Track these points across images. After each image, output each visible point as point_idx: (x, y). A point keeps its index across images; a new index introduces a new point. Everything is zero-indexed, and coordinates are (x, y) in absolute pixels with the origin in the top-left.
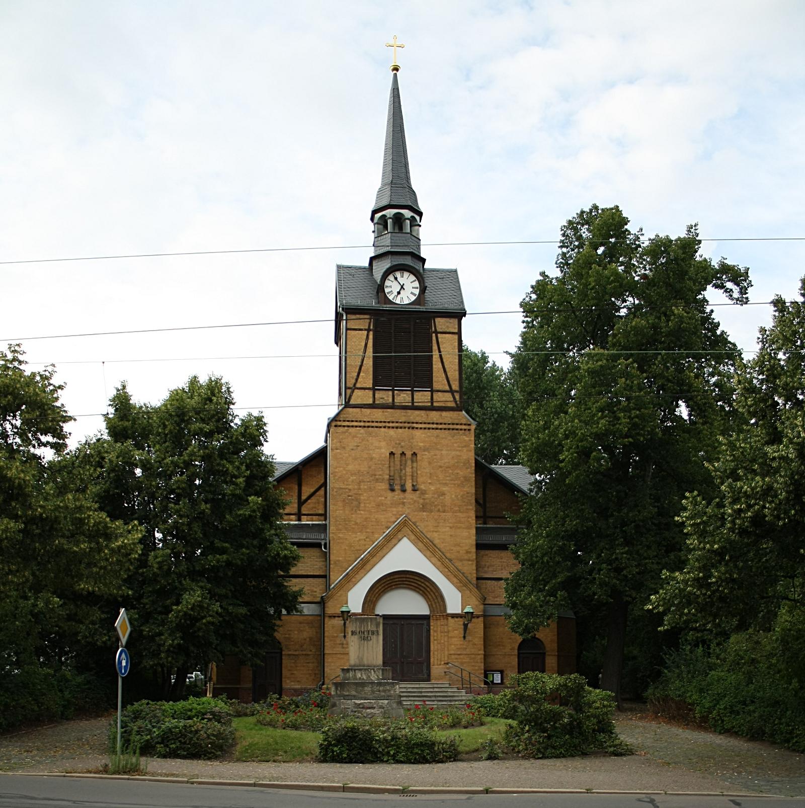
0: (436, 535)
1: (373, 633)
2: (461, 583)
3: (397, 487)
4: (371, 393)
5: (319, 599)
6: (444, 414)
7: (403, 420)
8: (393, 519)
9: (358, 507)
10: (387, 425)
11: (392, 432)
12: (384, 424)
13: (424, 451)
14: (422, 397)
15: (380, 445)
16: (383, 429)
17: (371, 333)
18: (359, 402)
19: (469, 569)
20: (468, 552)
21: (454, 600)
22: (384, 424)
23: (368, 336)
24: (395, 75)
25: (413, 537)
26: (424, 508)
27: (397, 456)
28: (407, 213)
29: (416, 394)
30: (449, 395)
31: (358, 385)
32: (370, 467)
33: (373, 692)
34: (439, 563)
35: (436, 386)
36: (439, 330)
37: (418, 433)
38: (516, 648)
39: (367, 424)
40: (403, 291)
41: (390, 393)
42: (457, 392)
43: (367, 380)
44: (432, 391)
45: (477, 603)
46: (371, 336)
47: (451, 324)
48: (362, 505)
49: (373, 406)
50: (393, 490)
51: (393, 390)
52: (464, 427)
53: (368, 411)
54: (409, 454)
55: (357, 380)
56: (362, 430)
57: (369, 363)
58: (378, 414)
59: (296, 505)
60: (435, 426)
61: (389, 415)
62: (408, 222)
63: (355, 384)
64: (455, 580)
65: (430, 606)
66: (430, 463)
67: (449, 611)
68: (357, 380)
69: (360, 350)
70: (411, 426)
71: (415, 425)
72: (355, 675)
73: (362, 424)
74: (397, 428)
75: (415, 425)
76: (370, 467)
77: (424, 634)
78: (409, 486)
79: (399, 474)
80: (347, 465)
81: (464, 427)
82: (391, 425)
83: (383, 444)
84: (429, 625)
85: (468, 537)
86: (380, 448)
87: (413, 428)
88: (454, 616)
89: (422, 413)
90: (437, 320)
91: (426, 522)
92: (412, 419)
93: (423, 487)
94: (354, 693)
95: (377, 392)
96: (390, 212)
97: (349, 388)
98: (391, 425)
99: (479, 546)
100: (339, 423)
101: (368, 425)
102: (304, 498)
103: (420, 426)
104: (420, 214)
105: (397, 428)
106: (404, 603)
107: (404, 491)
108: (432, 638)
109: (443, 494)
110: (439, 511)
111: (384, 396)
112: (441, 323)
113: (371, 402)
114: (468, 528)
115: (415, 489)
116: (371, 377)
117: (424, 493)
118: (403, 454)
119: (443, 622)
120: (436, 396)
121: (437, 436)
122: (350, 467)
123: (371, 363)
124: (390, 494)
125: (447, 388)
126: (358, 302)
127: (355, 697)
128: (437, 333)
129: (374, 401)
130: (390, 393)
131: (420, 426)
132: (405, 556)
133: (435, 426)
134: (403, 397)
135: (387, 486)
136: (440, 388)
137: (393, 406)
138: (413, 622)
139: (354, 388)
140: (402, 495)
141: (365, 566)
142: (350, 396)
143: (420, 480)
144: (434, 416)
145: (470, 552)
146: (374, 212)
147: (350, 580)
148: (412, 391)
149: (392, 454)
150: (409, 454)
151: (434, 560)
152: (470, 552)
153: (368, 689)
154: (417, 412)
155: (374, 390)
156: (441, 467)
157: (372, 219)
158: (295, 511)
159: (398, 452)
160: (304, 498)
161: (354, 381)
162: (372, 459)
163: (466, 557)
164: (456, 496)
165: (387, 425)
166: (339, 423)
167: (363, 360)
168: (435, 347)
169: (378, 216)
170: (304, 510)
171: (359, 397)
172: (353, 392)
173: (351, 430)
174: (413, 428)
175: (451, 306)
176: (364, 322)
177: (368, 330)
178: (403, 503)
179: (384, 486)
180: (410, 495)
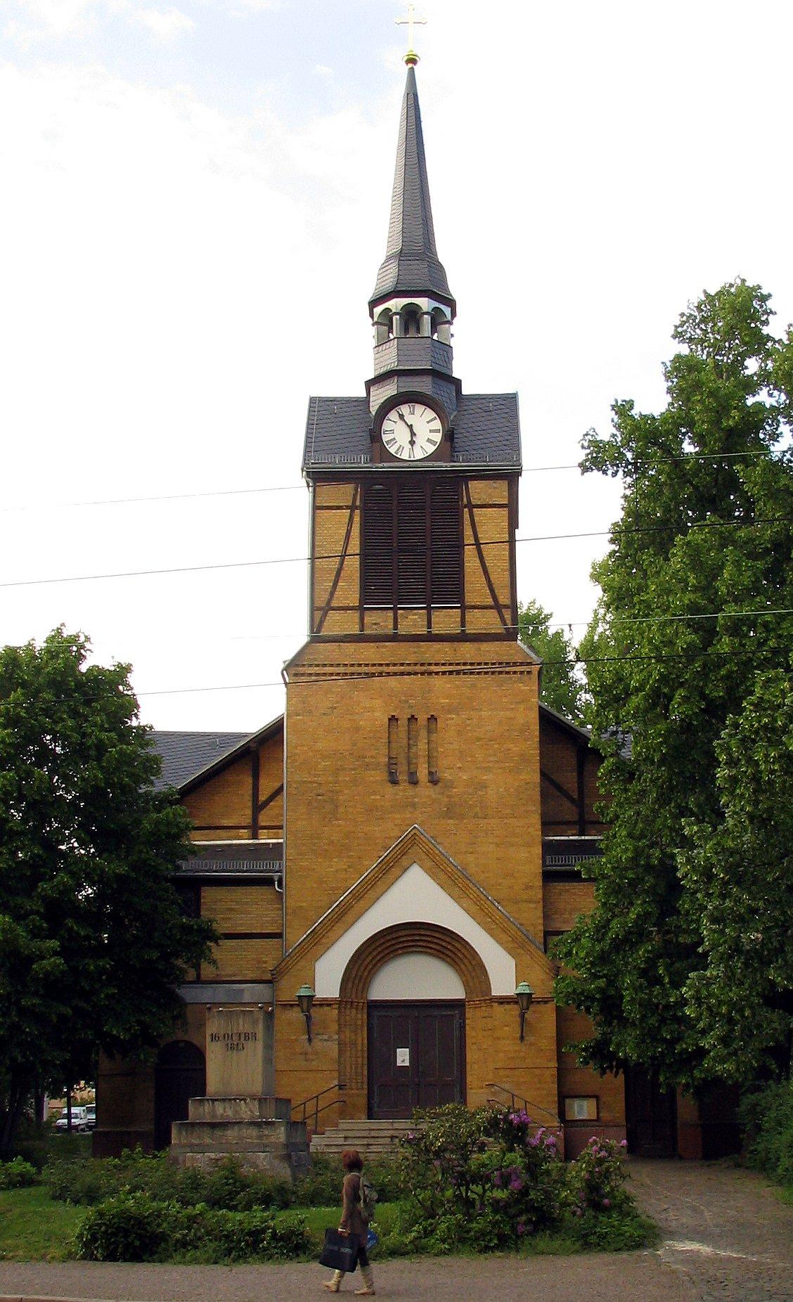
0: (471, 858)
1: (247, 1037)
2: (514, 943)
3: (403, 777)
4: (357, 615)
5: (268, 977)
6: (485, 646)
8: (396, 833)
10: (385, 669)
11: (393, 682)
12: (380, 669)
13: (450, 712)
14: (446, 620)
15: (373, 706)
17: (357, 512)
18: (336, 631)
19: (532, 917)
20: (528, 887)
21: (503, 976)
22: (380, 669)
24: (412, 71)
25: (429, 864)
26: (449, 812)
27: (403, 723)
28: (424, 303)
29: (435, 614)
30: (494, 613)
34: (474, 908)
35: (470, 599)
36: (474, 502)
37: (438, 682)
40: (414, 437)
41: (390, 614)
42: (506, 607)
43: (350, 592)
44: (463, 608)
45: (543, 976)
46: (357, 519)
47: (497, 492)
48: (341, 810)
50: (394, 782)
51: (395, 610)
53: (350, 647)
54: (422, 718)
55: (332, 594)
58: (369, 652)
59: (249, 812)
61: (388, 652)
62: (427, 318)
64: (504, 937)
65: (466, 984)
66: (459, 733)
67: (497, 991)
68: (332, 594)
70: (425, 670)
71: (434, 668)
72: (214, 1110)
73: (341, 670)
74: (402, 674)
75: (434, 668)
77: (456, 1033)
78: (422, 774)
79: (406, 754)
82: (392, 669)
83: (377, 703)
85: (528, 860)
86: (372, 710)
87: (430, 673)
88: (503, 1001)
89: (446, 646)
90: (472, 484)
92: (428, 658)
93: (447, 775)
94: (208, 1141)
95: (367, 613)
96: (396, 304)
99: (549, 877)
100: (301, 670)
102: (262, 798)
104: (451, 303)
106: (416, 980)
107: (414, 782)
109: (484, 786)
110: (476, 816)
111: (380, 621)
112: (478, 490)
114: (528, 845)
115: (434, 780)
116: (357, 588)
117: (450, 785)
118: (413, 719)
119: (484, 1011)
120: (470, 615)
121: (474, 686)
122: (320, 746)
124: (390, 789)
125: (490, 601)
126: (337, 462)
128: (471, 507)
130: (390, 614)
132: (415, 898)
134: (413, 621)
135: (385, 776)
137: (463, 637)
138: (436, 1012)
139: (328, 608)
140: (411, 791)
141: (344, 916)
142: (322, 622)
143: (443, 762)
144: (467, 651)
146: (373, 304)
147: (319, 941)
148: (429, 609)
149: (393, 719)
150: (422, 718)
154: (437, 646)
155: (361, 610)
156: (479, 739)
157: (372, 315)
158: (247, 821)
159: (404, 717)
160: (262, 798)
161: (327, 596)
162: (357, 729)
163: (525, 897)
164: (506, 790)
165: (385, 669)
166: (301, 670)
168: (468, 532)
169: (378, 310)
170: (263, 820)
172: (325, 615)
174: (430, 673)
176: (345, 493)
177: (352, 508)
178: (414, 805)
179: (380, 775)
180: (425, 791)
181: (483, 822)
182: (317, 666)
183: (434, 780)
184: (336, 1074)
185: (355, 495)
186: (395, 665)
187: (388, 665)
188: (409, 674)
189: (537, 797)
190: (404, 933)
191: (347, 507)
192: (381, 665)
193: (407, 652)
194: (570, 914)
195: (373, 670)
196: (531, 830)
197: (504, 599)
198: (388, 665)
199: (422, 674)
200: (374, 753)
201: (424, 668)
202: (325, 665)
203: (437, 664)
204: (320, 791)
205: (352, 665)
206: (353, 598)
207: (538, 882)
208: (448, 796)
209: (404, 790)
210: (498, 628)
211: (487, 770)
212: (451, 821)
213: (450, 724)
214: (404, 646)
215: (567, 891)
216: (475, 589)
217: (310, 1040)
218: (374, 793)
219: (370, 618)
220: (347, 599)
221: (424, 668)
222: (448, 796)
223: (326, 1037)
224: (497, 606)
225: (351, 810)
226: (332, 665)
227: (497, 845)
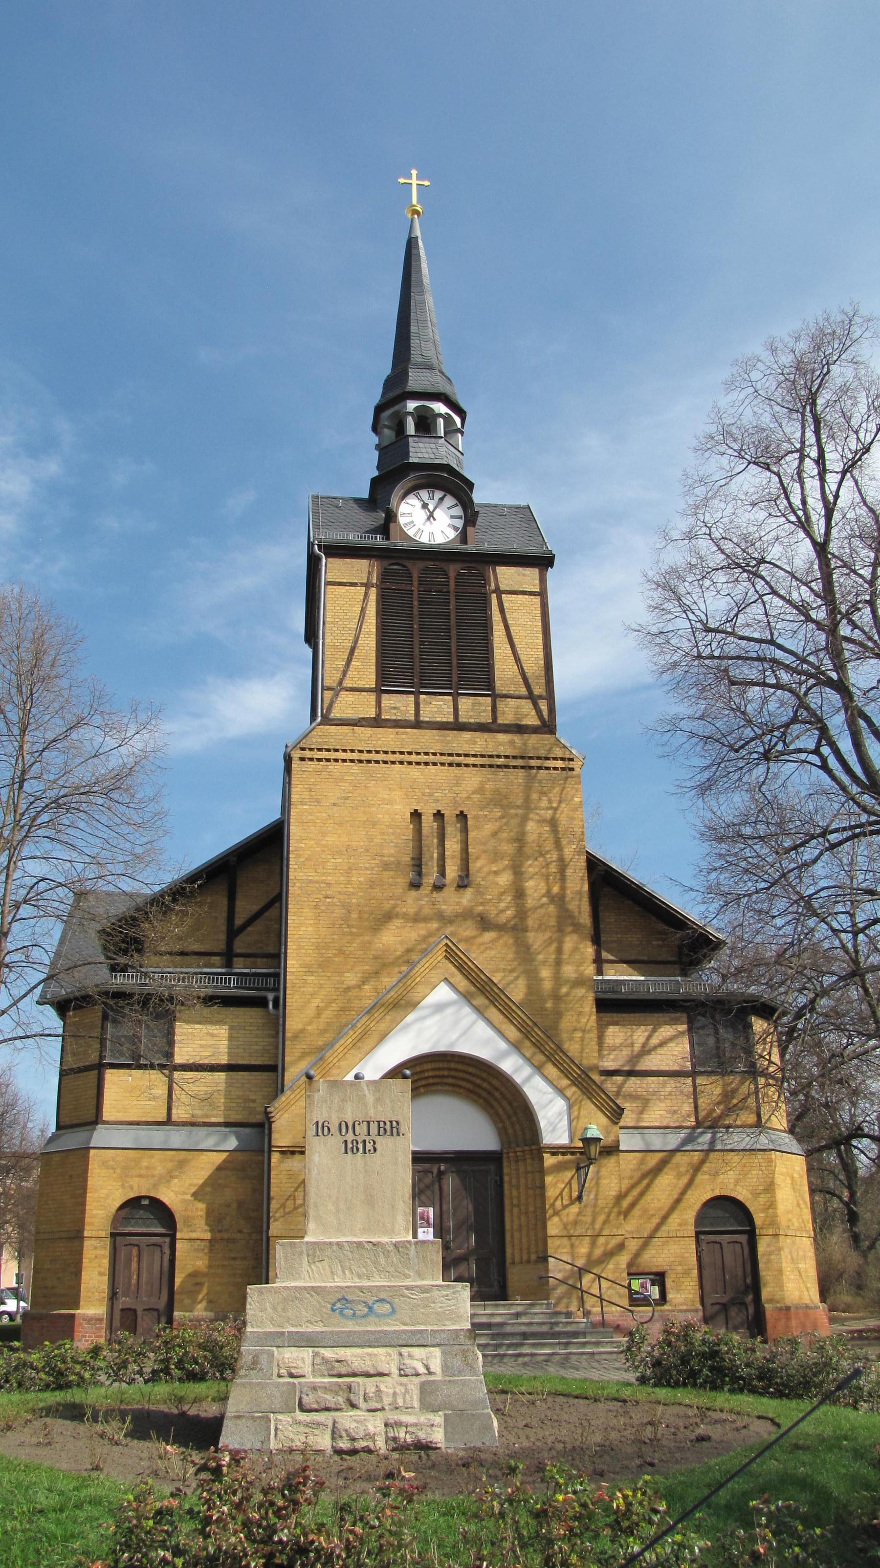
4: (372, 697)
7: (437, 748)
10: (406, 757)
11: (415, 772)
14: (474, 708)
16: (398, 766)
17: (373, 591)
18: (350, 714)
22: (398, 757)
23: (366, 595)
28: (440, 408)
31: (347, 683)
32: (371, 840)
35: (500, 686)
36: (503, 587)
38: (692, 1221)
41: (411, 698)
42: (541, 697)
47: (528, 577)
49: (377, 722)
51: (417, 694)
53: (368, 731)
55: (344, 673)
56: (355, 768)
57: (369, 643)
58: (387, 738)
59: (223, 937)
61: (410, 739)
63: (341, 682)
65: (502, 1132)
68: (344, 673)
73: (355, 756)
74: (426, 764)
76: (371, 840)
80: (324, 834)
82: (414, 758)
83: (397, 795)
86: (390, 802)
90: (501, 570)
95: (385, 696)
97: (329, 689)
98: (414, 758)
100: (308, 754)
101: (367, 759)
102: (239, 921)
108: (507, 1202)
111: (399, 705)
112: (507, 576)
120: (501, 705)
122: (330, 839)
128: (499, 592)
130: (411, 698)
134: (437, 707)
136: (512, 690)
139: (340, 688)
146: (379, 410)
149: (416, 815)
154: (467, 735)
155: (379, 691)
158: (221, 946)
160: (239, 921)
161: (339, 675)
162: (374, 824)
165: (406, 757)
166: (308, 754)
167: (356, 641)
168: (496, 617)
170: (240, 946)
172: (337, 695)
173: (332, 766)
177: (367, 585)
185: (370, 573)
191: (362, 584)
193: (429, 740)
198: (410, 753)
203: (466, 755)
206: (370, 680)
219: (388, 701)
224: (531, 697)
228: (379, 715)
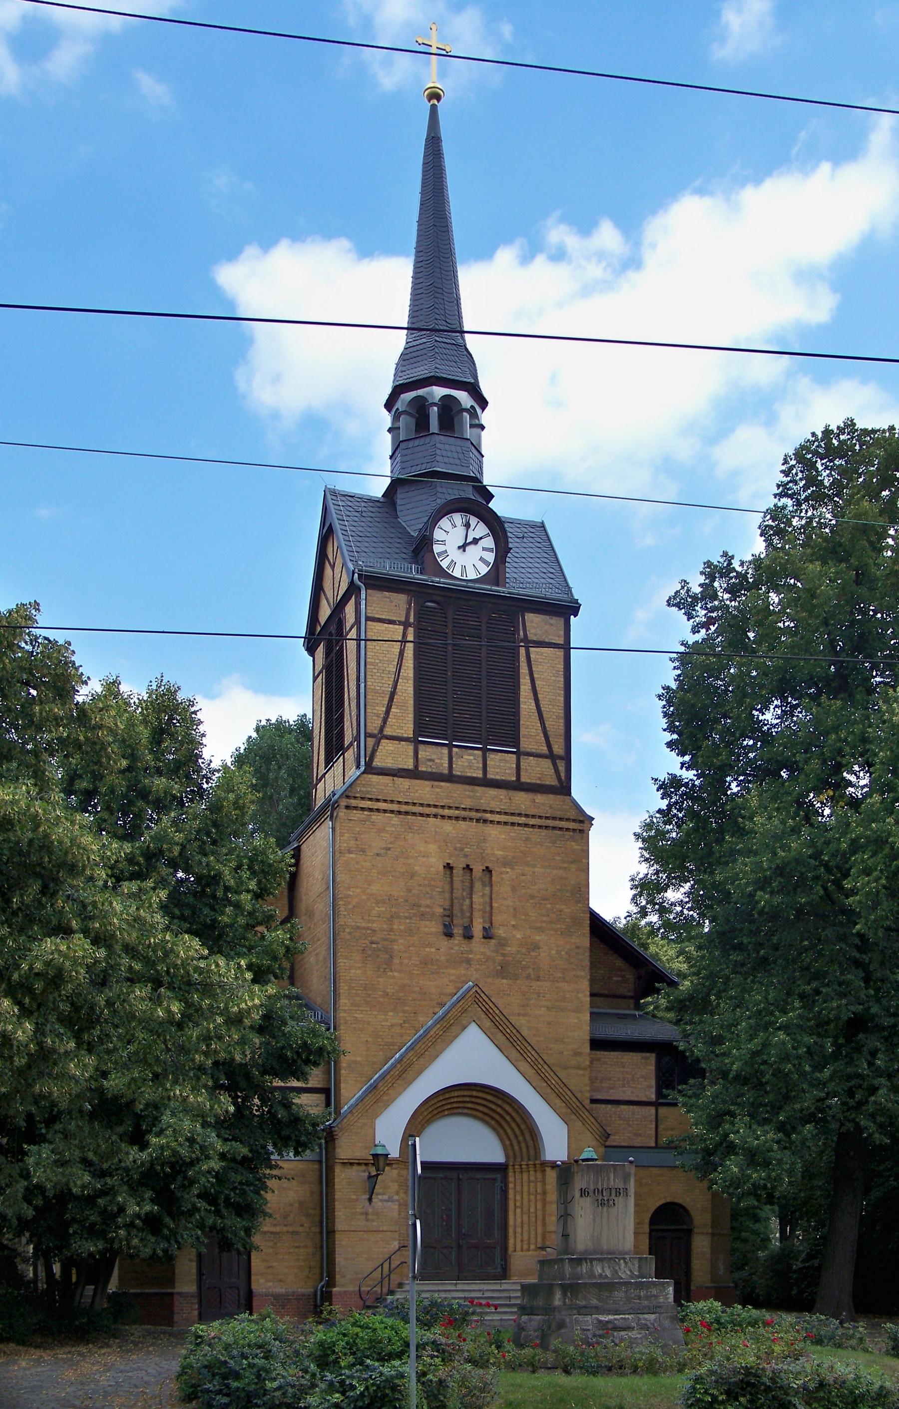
3: (457, 931)
4: (410, 748)
6: (540, 798)
7: (468, 803)
8: (450, 989)
9: (389, 963)
10: (440, 811)
11: (448, 827)
13: (505, 865)
14: (501, 765)
16: (432, 820)
17: (411, 630)
19: (579, 1083)
20: (577, 1054)
21: (556, 1139)
25: (487, 1023)
26: (503, 971)
29: (491, 757)
31: (388, 731)
32: (410, 891)
33: (628, 1299)
34: (531, 1072)
35: (526, 744)
36: (531, 637)
37: (493, 832)
38: (647, 1221)
39: (404, 808)
41: (445, 751)
42: (560, 758)
44: (518, 754)
49: (414, 774)
50: (449, 935)
51: (450, 746)
52: (572, 825)
53: (404, 783)
55: (385, 721)
56: (395, 819)
57: (407, 688)
58: (423, 791)
60: (522, 820)
66: (514, 889)
68: (385, 721)
69: (390, 662)
70: (480, 816)
71: (488, 816)
73: (395, 807)
74: (457, 818)
75: (488, 816)
76: (410, 891)
78: (477, 930)
81: (572, 825)
82: (446, 812)
83: (433, 848)
84: (505, 1179)
86: (426, 855)
87: (485, 821)
88: (553, 1165)
89: (501, 793)
90: (530, 617)
91: (507, 996)
92: (483, 803)
95: (421, 747)
97: (372, 736)
98: (446, 812)
99: (597, 1044)
100: (353, 802)
101: (405, 810)
103: (497, 818)
105: (457, 818)
106: (469, 1142)
107: (468, 937)
108: (511, 1204)
109: (536, 947)
110: (528, 977)
111: (435, 757)
112: (536, 625)
113: (411, 767)
115: (488, 935)
116: (411, 717)
117: (503, 943)
118: (468, 868)
120: (526, 762)
121: (527, 839)
122: (374, 888)
123: (411, 690)
124: (444, 943)
125: (544, 749)
127: (598, 1310)
129: (416, 766)
130: (445, 751)
131: (497, 818)
132: (472, 1058)
133: (522, 820)
134: (468, 762)
135: (440, 929)
139: (380, 736)
141: (404, 1072)
142: (374, 752)
143: (497, 919)
144: (522, 801)
145: (580, 1054)
148: (485, 751)
149: (449, 867)
150: (478, 868)
151: (523, 1065)
152: (580, 1054)
153: (619, 1295)
154: (492, 792)
155: (415, 742)
156: (532, 897)
159: (459, 865)
161: (379, 722)
162: (413, 875)
164: (558, 952)
165: (440, 811)
166: (353, 802)
167: (395, 686)
168: (524, 670)
171: (392, 755)
172: (378, 744)
173: (375, 817)
174: (485, 821)
175: (552, 594)
177: (406, 624)
178: (468, 961)
179: (434, 927)
180: (478, 945)
181: (535, 984)
182: (370, 799)
183: (488, 935)
184: (396, 1235)
185: (408, 610)
186: (450, 808)
187: (443, 807)
188: (464, 819)
189: (587, 962)
190: (456, 1094)
191: (400, 623)
192: (435, 806)
194: (601, 1082)
195: (427, 810)
196: (580, 995)
197: (558, 749)
198: (443, 807)
199: (478, 820)
200: (428, 902)
201: (479, 815)
202: (378, 800)
203: (492, 812)
204: (374, 939)
205: (407, 803)
206: (408, 730)
207: (587, 1049)
208: (503, 955)
209: (459, 945)
210: (552, 781)
211: (540, 930)
212: (505, 981)
213: (504, 877)
214: (460, 788)
215: (599, 1060)
216: (530, 734)
217: (370, 1200)
218: (430, 945)
219: (424, 753)
220: (401, 728)
221: (479, 815)
222: (503, 955)
223: (386, 1197)
224: (551, 756)
225: (406, 961)
226: (385, 801)
227: (549, 1009)
228: (416, 766)
